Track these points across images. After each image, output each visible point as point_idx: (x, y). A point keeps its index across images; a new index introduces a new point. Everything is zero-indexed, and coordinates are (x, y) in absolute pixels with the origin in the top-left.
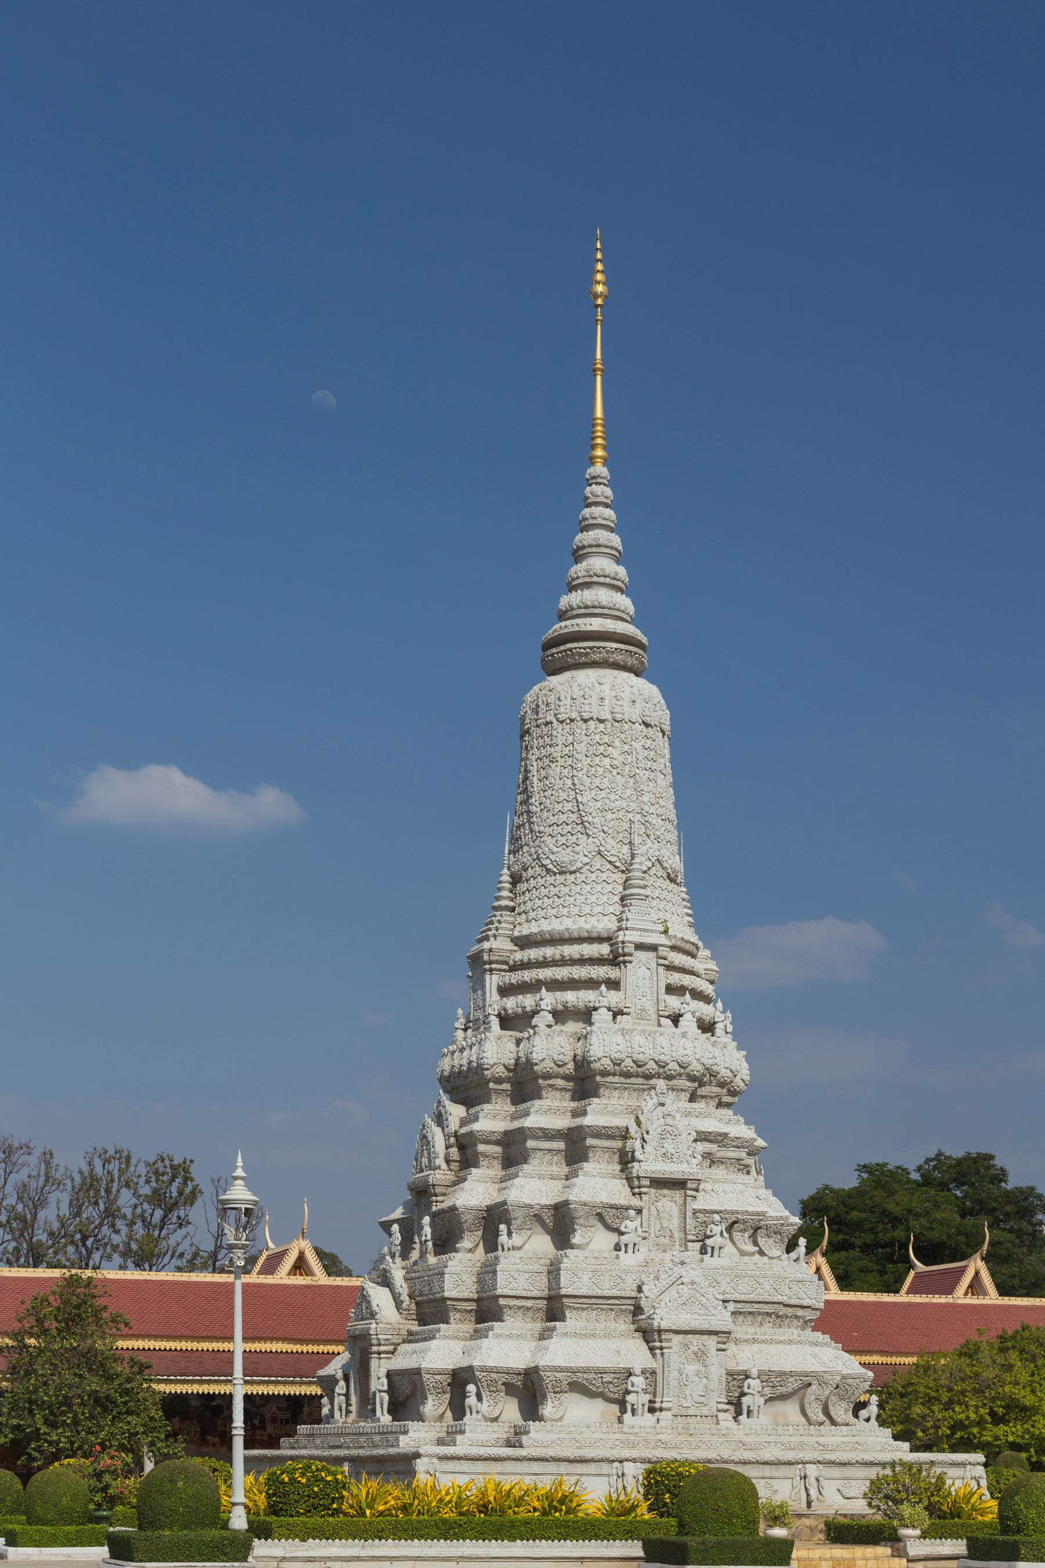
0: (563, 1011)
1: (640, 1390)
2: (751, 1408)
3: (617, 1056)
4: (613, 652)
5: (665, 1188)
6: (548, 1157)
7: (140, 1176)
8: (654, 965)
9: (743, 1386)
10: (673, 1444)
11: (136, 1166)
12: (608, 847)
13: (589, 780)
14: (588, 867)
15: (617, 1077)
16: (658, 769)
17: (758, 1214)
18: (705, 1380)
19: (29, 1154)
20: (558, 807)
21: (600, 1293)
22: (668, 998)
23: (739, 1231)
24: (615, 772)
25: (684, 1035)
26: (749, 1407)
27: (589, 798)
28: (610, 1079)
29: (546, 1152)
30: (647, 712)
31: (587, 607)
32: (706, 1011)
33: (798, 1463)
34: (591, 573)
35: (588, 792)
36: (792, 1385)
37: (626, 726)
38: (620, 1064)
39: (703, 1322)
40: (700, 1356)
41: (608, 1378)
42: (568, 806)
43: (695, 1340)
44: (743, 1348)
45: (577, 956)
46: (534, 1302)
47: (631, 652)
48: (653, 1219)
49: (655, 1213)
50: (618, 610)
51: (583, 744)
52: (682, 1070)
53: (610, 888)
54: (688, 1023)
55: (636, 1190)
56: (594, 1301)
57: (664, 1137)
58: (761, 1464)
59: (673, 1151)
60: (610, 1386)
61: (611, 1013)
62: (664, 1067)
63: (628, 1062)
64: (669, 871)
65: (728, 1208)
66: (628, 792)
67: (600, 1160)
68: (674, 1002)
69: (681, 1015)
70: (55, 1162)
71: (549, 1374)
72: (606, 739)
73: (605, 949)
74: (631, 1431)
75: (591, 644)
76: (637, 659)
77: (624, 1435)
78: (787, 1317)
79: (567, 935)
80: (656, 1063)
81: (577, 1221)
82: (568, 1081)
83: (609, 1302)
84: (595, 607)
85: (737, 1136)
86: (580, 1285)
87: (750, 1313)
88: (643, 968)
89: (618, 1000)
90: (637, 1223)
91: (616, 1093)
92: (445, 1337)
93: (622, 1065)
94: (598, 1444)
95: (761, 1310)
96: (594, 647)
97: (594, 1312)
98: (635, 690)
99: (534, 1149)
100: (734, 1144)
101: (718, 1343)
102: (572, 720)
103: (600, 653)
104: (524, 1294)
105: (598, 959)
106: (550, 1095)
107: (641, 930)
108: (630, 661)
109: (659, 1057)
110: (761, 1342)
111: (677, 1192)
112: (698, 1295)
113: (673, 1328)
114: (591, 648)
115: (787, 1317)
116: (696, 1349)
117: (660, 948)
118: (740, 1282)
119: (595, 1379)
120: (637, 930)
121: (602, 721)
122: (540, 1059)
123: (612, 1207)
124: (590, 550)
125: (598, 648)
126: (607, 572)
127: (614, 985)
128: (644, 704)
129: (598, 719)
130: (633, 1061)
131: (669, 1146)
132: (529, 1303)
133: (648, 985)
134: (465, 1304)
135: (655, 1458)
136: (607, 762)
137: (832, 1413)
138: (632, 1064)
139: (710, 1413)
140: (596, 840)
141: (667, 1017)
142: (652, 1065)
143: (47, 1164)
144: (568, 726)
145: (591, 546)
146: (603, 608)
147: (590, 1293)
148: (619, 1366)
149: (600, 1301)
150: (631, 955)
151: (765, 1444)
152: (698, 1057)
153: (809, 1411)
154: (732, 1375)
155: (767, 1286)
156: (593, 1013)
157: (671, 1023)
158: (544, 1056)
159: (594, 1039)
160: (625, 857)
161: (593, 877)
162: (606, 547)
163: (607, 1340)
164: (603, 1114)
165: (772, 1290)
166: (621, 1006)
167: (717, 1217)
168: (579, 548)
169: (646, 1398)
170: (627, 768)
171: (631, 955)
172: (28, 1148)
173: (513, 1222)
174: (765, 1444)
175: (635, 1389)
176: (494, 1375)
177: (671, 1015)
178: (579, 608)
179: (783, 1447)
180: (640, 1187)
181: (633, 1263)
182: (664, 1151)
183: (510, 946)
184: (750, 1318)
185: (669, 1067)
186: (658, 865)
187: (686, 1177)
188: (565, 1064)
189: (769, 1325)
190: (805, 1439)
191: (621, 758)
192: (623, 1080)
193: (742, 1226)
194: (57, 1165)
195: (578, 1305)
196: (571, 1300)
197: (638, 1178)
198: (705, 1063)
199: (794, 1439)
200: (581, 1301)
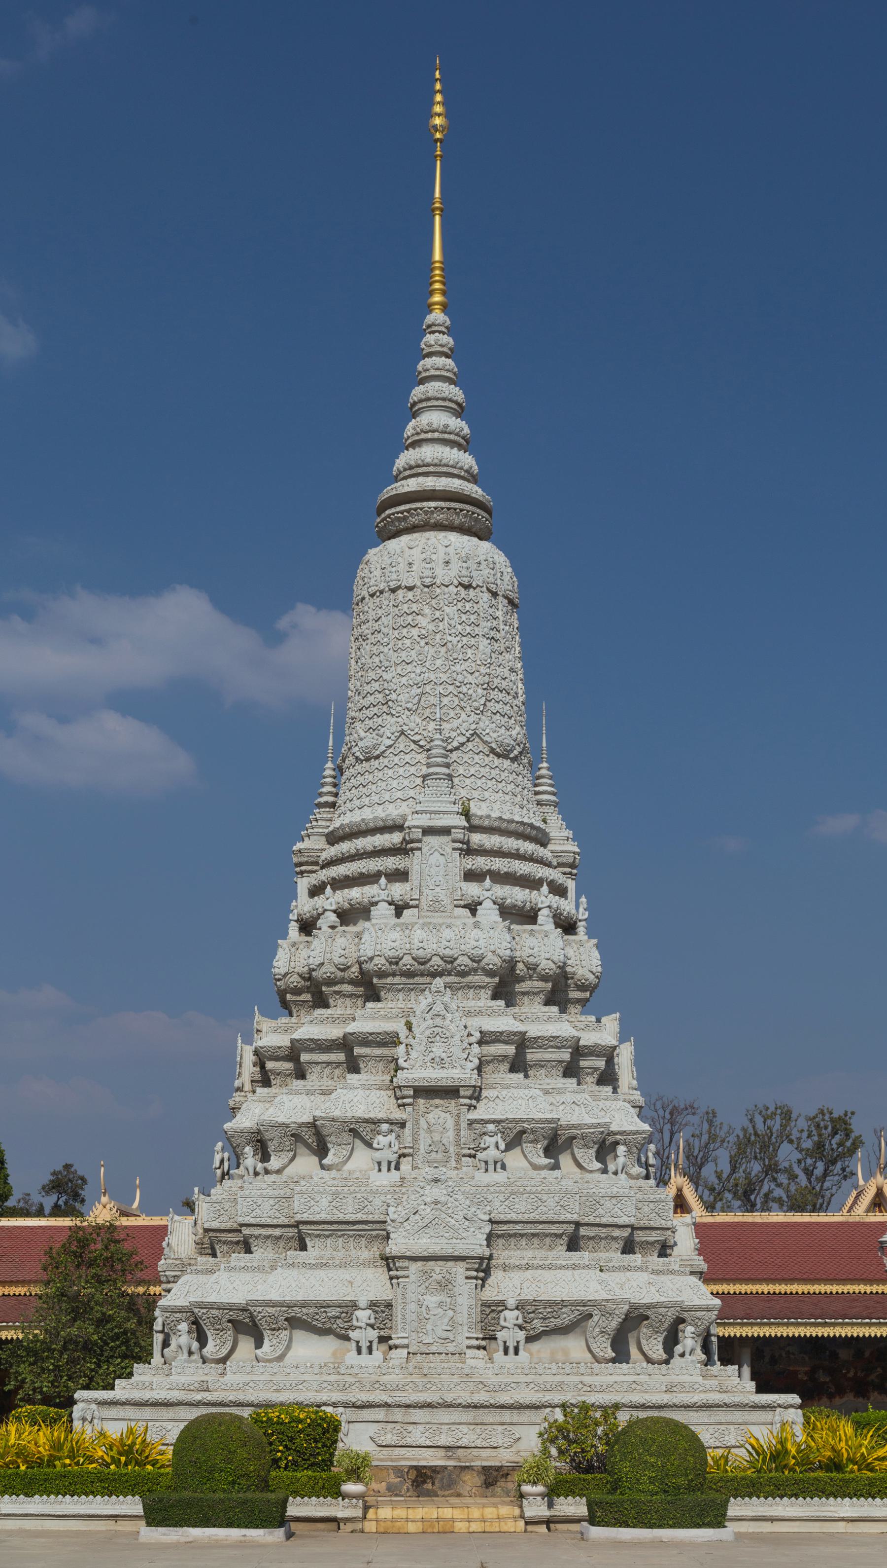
0: (350, 910)
1: (363, 1325)
3: (391, 953)
4: (432, 512)
5: (436, 1098)
6: (327, 1071)
7: (802, 1131)
8: (449, 850)
9: (499, 1318)
10: (394, 1386)
11: (796, 1120)
12: (412, 725)
13: (396, 654)
14: (391, 750)
15: (398, 978)
16: (480, 634)
17: (548, 1121)
18: (451, 1313)
19: (694, 1114)
20: (367, 688)
21: (341, 1217)
22: (465, 885)
23: (531, 1142)
24: (423, 643)
25: (476, 925)
26: (505, 1342)
27: (394, 674)
28: (389, 980)
29: (324, 1065)
30: (464, 572)
31: (411, 468)
32: (517, 895)
33: (546, 1407)
34: (418, 430)
35: (393, 668)
36: (567, 1317)
37: (438, 591)
38: (397, 963)
39: (446, 1246)
40: (445, 1285)
41: (333, 1312)
42: (376, 686)
43: (437, 1267)
44: (513, 1275)
45: (370, 848)
46: (283, 1230)
47: (455, 509)
48: (422, 1134)
49: (425, 1126)
50: (447, 465)
51: (390, 617)
52: (475, 965)
53: (413, 770)
54: (489, 913)
55: (399, 1101)
57: (433, 1040)
58: (497, 1407)
59: (444, 1055)
60: (339, 1321)
61: (393, 907)
62: (452, 962)
63: (407, 960)
64: (494, 745)
65: (510, 1116)
66: (438, 662)
67: (374, 1071)
68: (473, 890)
69: (480, 904)
70: (717, 1121)
71: (260, 1309)
72: (415, 607)
73: (396, 838)
74: (349, 1371)
75: (407, 506)
76: (466, 516)
77: (341, 1377)
78: (601, 1239)
79: (363, 827)
80: (442, 959)
81: (329, 1139)
82: (356, 986)
83: (354, 1228)
84: (419, 466)
85: (553, 1035)
86: (317, 1209)
87: (534, 1235)
88: (436, 853)
89: (403, 892)
90: (392, 1137)
91: (401, 995)
92: (198, 1272)
93: (401, 963)
94: (301, 1387)
95: (546, 1232)
96: (411, 509)
97: (340, 1240)
98: (451, 550)
99: (310, 1063)
100: (552, 1044)
101: (468, 1269)
102: (382, 592)
103: (418, 515)
104: (269, 1221)
105: (390, 849)
106: (339, 1002)
107: (431, 813)
108: (457, 520)
109: (444, 951)
110: (537, 1268)
111: (453, 1101)
112: (443, 1216)
113: (407, 1254)
114: (408, 511)
115: (601, 1239)
116: (439, 1277)
117: (453, 830)
118: (517, 1200)
119: (317, 1314)
120: (426, 812)
121: (410, 589)
122: (317, 963)
123: (367, 1121)
124: (420, 405)
125: (415, 510)
126: (435, 426)
127: (401, 876)
128: (460, 563)
129: (406, 587)
130: (413, 958)
131: (438, 1050)
132: (277, 1232)
133: (442, 873)
134: (230, 1235)
135: (359, 1402)
136: (415, 632)
137: (645, 1348)
138: (413, 962)
139: (458, 1350)
140: (399, 719)
141: (464, 907)
142: (436, 961)
143: (711, 1123)
144: (378, 599)
145: (421, 401)
146: (428, 465)
147: (329, 1218)
148: (344, 1299)
149: (343, 1227)
150: (420, 841)
151: (512, 1385)
152: (492, 948)
153: (594, 1347)
154: (489, 1306)
155: (551, 1203)
156: (372, 908)
157: (469, 914)
158: (321, 960)
159: (366, 937)
160: (430, 734)
161: (396, 759)
162: (437, 399)
163: (342, 1270)
164: (373, 1018)
165: (559, 1208)
166: (407, 898)
167: (491, 1127)
168: (414, 404)
169: (373, 1334)
170: (438, 636)
171: (420, 841)
172: (691, 1109)
173: (269, 1143)
174: (512, 1385)
175: (359, 1324)
176: (215, 1312)
177: (470, 904)
178: (405, 470)
179: (536, 1389)
180: (403, 1098)
181: (385, 1183)
182: (432, 1055)
183: (321, 843)
184: (536, 1241)
185: (458, 962)
186: (477, 740)
187: (456, 1084)
188: (349, 967)
189: (560, 1248)
190: (566, 1379)
191: (431, 627)
192: (404, 980)
193: (531, 1136)
194: (721, 1124)
195: (318, 1232)
196: (308, 1227)
197: (399, 1087)
198: (501, 954)
199: (550, 1379)
200: (320, 1227)
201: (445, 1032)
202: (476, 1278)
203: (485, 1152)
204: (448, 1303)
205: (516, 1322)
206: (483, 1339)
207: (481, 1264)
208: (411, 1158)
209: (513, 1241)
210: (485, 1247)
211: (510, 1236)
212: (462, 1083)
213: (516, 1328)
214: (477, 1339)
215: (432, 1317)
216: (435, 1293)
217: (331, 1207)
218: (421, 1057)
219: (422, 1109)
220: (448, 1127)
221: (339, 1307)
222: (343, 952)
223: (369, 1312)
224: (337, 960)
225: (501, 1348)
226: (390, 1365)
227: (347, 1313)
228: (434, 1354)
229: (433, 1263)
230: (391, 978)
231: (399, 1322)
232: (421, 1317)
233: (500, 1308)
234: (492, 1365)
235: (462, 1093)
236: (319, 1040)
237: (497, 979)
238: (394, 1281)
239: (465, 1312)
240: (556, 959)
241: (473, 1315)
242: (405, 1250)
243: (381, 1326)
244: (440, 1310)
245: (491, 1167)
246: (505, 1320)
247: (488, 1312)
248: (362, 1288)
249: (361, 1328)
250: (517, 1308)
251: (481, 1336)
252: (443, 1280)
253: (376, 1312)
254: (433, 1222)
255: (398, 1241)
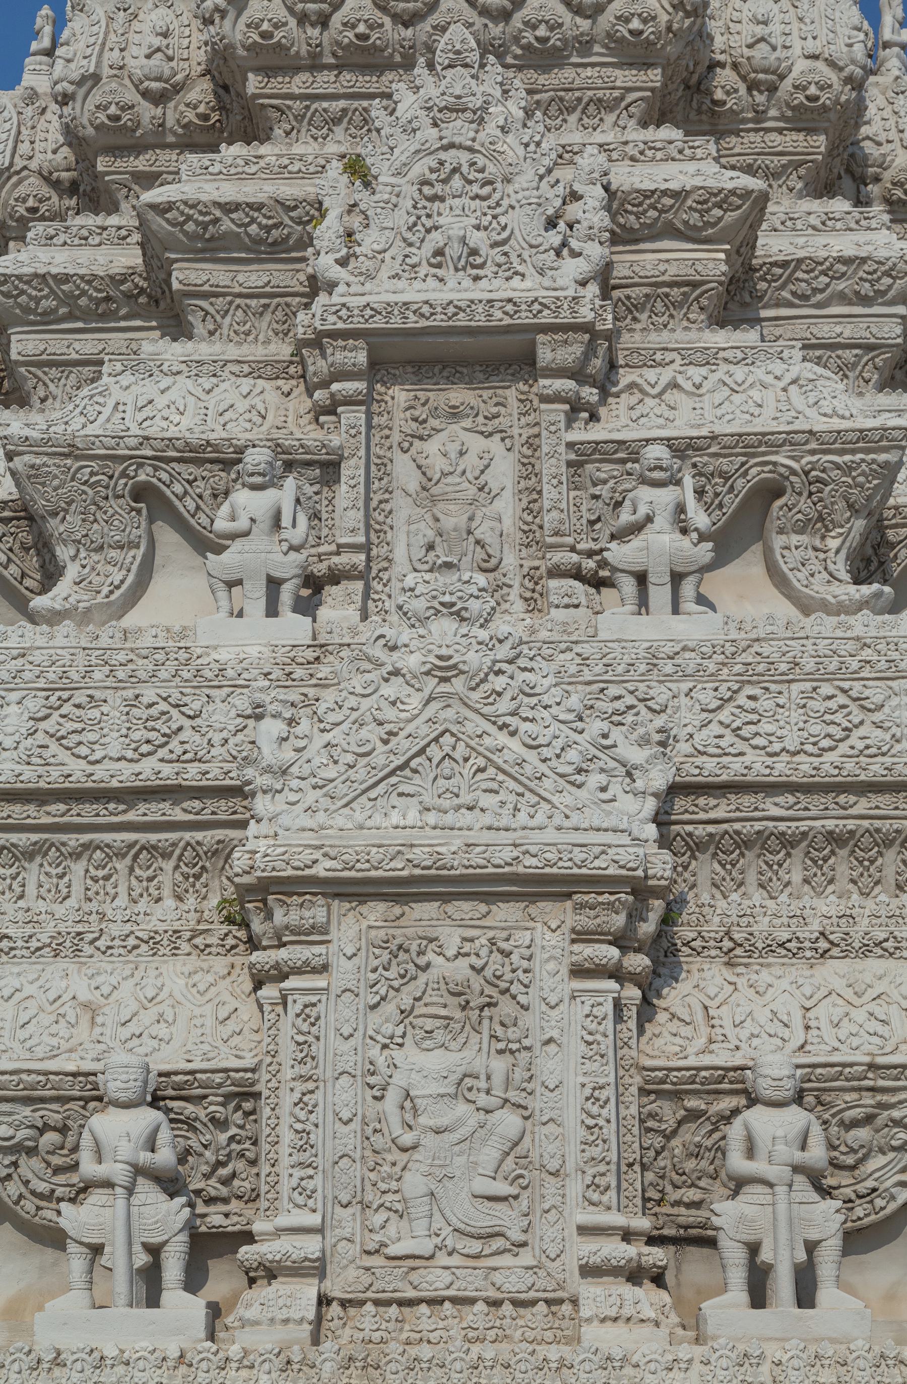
1: (118, 1172)
2: (765, 1255)
26: (753, 1249)
28: (298, 83)
44: (765, 976)
52: (584, 24)
56: (55, 812)
57: (438, 189)
59: (477, 239)
60: (29, 1166)
83: (131, 816)
87: (835, 839)
95: (885, 825)
97: (78, 868)
99: (40, 364)
100: (841, 285)
101: (581, 936)
110: (865, 951)
111: (511, 394)
113: (319, 871)
116: (460, 970)
118: (765, 704)
149: (87, 813)
163: (62, 964)
182: (436, 239)
187: (525, 318)
188: (178, 89)
193: (804, 504)
201: (481, 161)
202: (616, 974)
203: (636, 542)
204: (498, 1080)
205: (799, 1156)
206: (652, 1241)
207: (635, 915)
208: (359, 585)
209: (751, 863)
210: (653, 848)
211: (744, 844)
212: (546, 318)
213: (801, 1181)
214: (627, 1236)
215: (429, 1140)
216: (440, 1036)
217: (41, 738)
218: (398, 249)
219: (401, 422)
220: (494, 486)
221: (27, 1101)
222: (157, 41)
223: (149, 1116)
224: (138, 64)
225: (737, 1276)
226: (234, 1351)
227: (63, 1130)
228: (433, 1302)
229: (429, 909)
230: (304, 76)
231: (285, 1161)
232: (378, 1141)
233: (725, 1104)
234: (698, 1351)
235: (545, 355)
236: (66, 278)
237: (655, 76)
238: (269, 992)
239: (572, 1117)
240: (838, 51)
241: (610, 1131)
242: (307, 856)
243: (213, 1187)
244: (462, 1108)
245: (660, 595)
246: (750, 1152)
247: (669, 1125)
248: (133, 1028)
249: (108, 1184)
250: (798, 1098)
251: (643, 1223)
252: (477, 983)
253: (190, 1124)
254: (435, 752)
255: (285, 820)
